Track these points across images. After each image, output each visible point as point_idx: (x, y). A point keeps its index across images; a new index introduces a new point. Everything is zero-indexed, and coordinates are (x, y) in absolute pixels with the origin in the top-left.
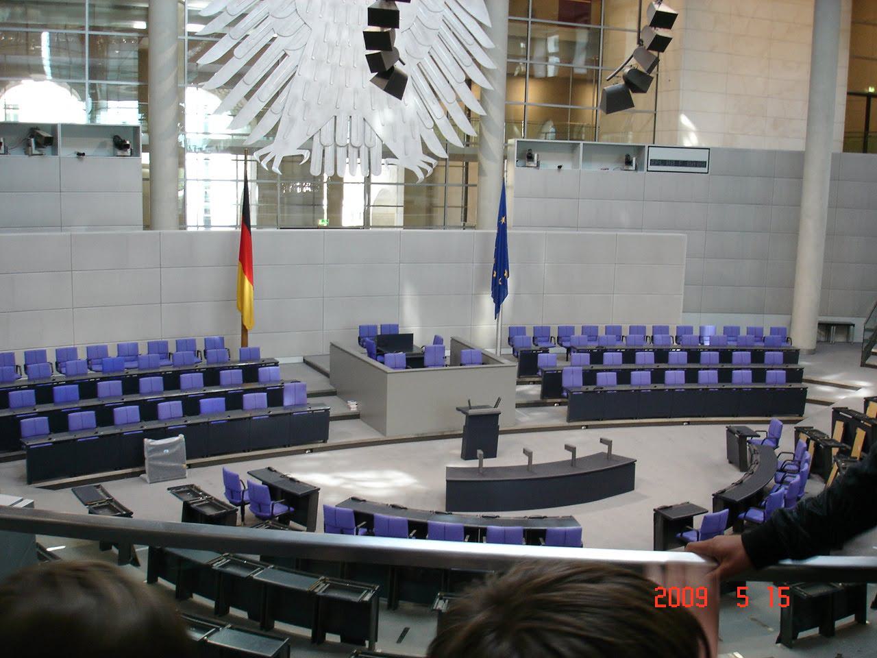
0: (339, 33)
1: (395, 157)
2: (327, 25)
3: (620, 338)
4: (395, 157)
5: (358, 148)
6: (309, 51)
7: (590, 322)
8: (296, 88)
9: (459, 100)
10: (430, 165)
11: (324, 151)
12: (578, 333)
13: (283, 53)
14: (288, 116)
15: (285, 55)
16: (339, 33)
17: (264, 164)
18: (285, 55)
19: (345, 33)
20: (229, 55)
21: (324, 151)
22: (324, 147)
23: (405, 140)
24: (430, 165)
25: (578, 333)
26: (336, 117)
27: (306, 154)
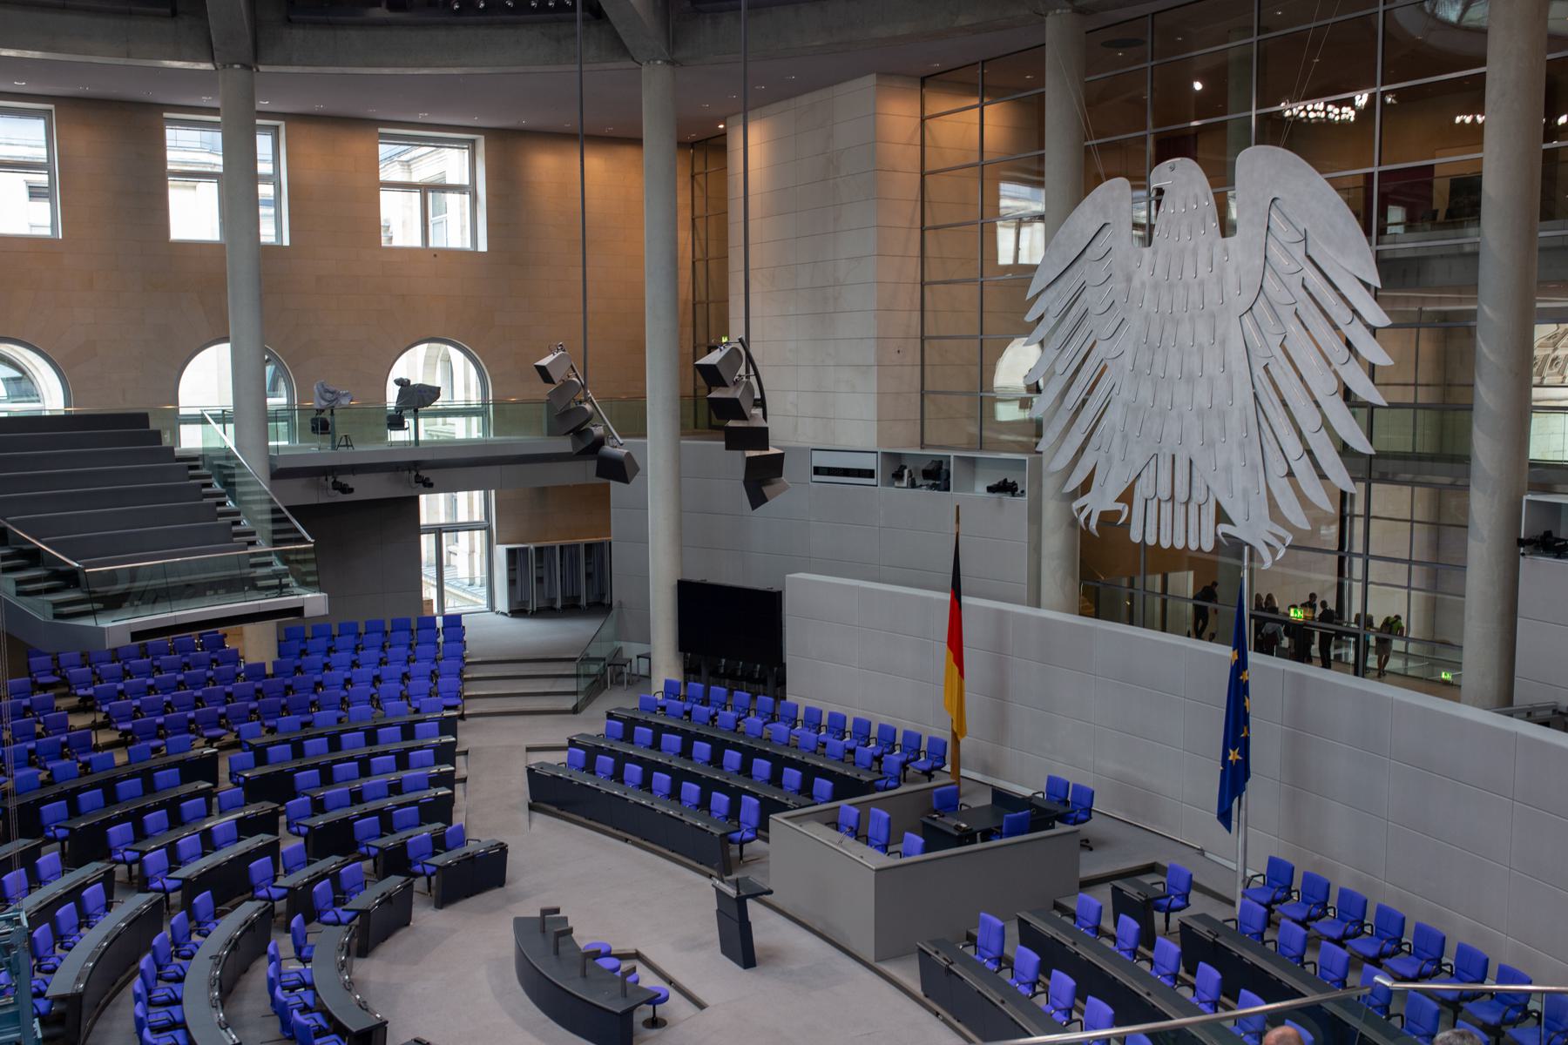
1: (1230, 522)
4: (1230, 522)
8: (1114, 416)
9: (1326, 424)
10: (1282, 540)
14: (1104, 454)
23: (1245, 492)
24: (1282, 540)
27: (1120, 506)
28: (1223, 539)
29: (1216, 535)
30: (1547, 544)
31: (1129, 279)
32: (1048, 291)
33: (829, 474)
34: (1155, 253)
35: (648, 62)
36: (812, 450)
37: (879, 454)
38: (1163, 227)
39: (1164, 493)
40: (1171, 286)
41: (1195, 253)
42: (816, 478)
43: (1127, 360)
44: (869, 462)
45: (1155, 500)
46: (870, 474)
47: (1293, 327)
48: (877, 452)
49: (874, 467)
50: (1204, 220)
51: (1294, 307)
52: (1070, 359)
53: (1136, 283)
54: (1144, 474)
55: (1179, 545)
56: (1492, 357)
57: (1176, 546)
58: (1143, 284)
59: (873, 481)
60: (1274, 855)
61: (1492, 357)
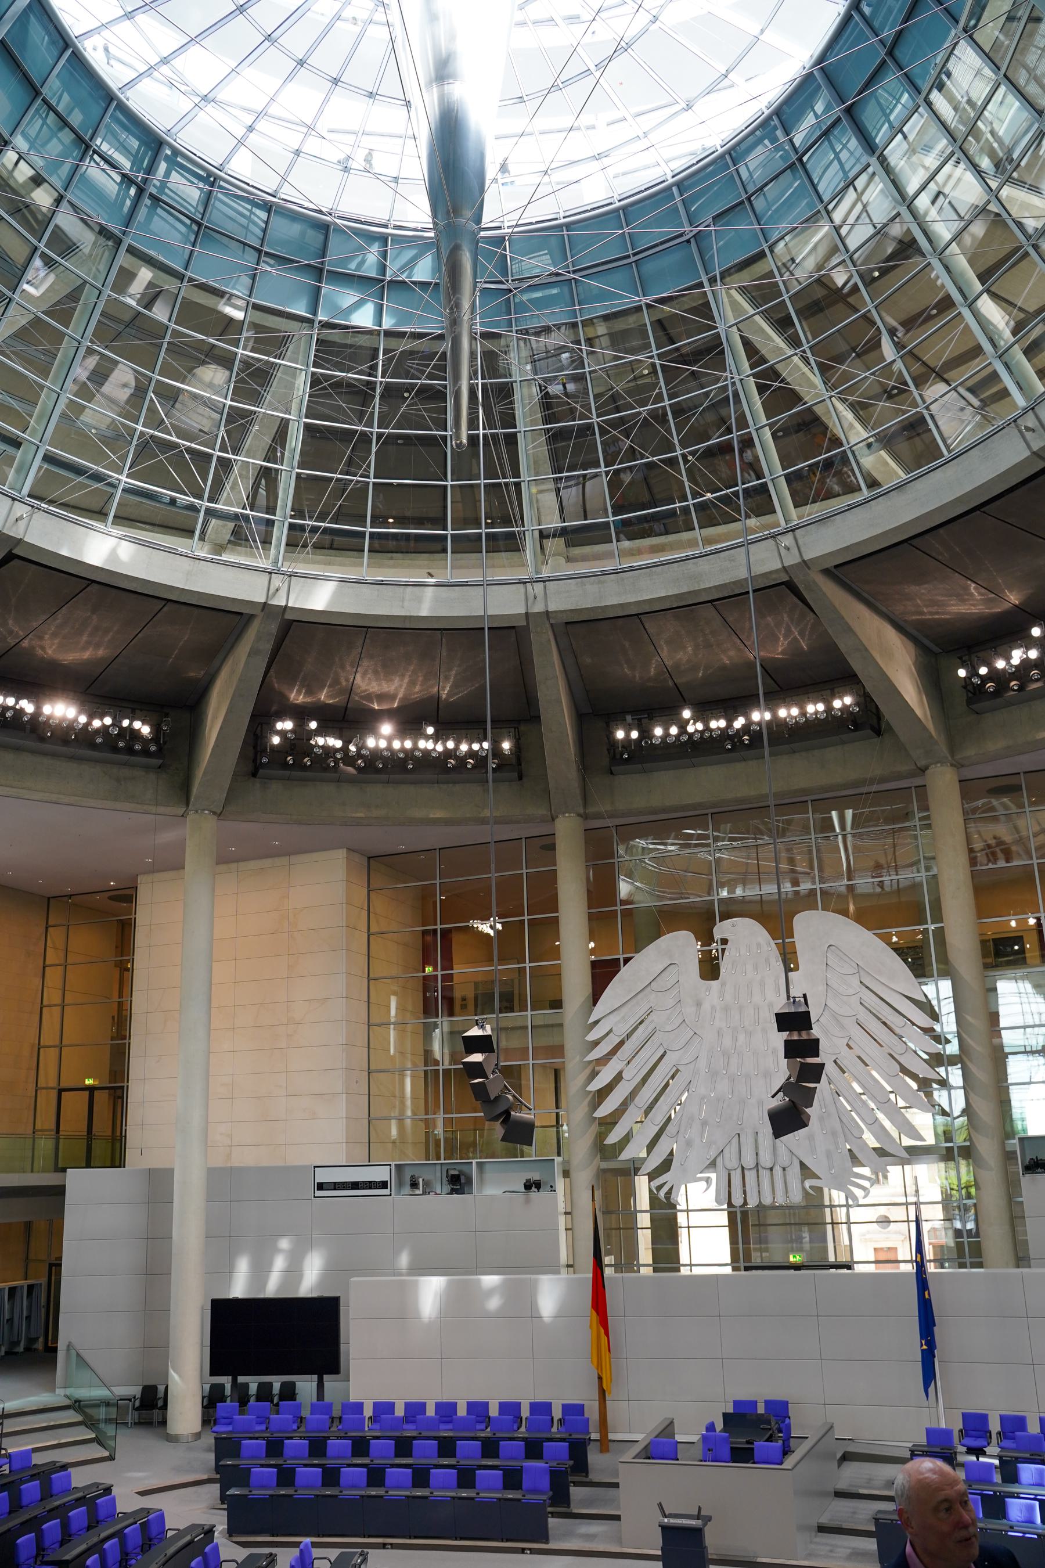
0: (735, 1039)
2: (719, 1032)
3: (487, 1419)
5: (771, 1169)
6: (702, 1063)
7: (477, 1397)
11: (729, 1175)
12: (430, 1411)
13: (675, 1069)
15: (678, 1071)
16: (735, 1039)
17: (662, 1194)
18: (678, 1071)
19: (742, 1038)
20: (618, 1078)
21: (729, 1175)
22: (729, 1170)
25: (430, 1411)
26: (739, 1134)
28: (811, 1191)
29: (804, 1189)
30: (1034, 1166)
31: (699, 1004)
32: (611, 1016)
33: (335, 1189)
34: (723, 984)
35: (197, 812)
36: (315, 1167)
37: (393, 1167)
38: (730, 966)
39: (749, 1161)
40: (726, 1009)
41: (762, 984)
42: (319, 1193)
43: (702, 1063)
44: (380, 1174)
45: (740, 1169)
46: (384, 1185)
47: (857, 1033)
48: (390, 1165)
49: (387, 1178)
50: (768, 961)
51: (855, 1018)
52: (639, 1067)
53: (706, 1006)
54: (726, 1151)
55: (767, 1201)
56: (979, 1048)
57: (763, 1203)
58: (713, 1008)
59: (386, 1192)
60: (929, 1426)
61: (979, 1048)
